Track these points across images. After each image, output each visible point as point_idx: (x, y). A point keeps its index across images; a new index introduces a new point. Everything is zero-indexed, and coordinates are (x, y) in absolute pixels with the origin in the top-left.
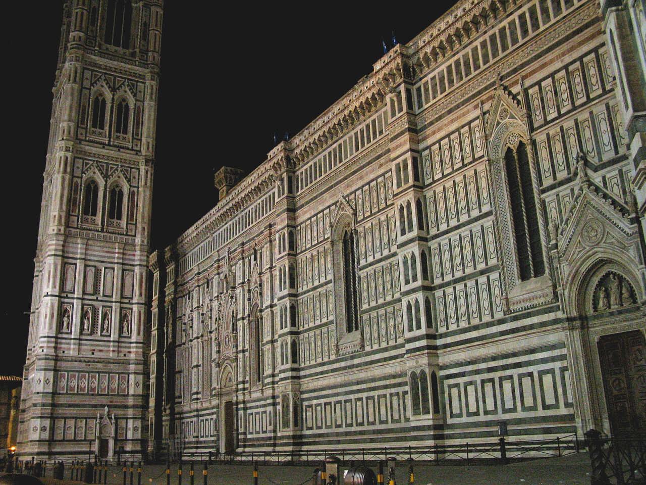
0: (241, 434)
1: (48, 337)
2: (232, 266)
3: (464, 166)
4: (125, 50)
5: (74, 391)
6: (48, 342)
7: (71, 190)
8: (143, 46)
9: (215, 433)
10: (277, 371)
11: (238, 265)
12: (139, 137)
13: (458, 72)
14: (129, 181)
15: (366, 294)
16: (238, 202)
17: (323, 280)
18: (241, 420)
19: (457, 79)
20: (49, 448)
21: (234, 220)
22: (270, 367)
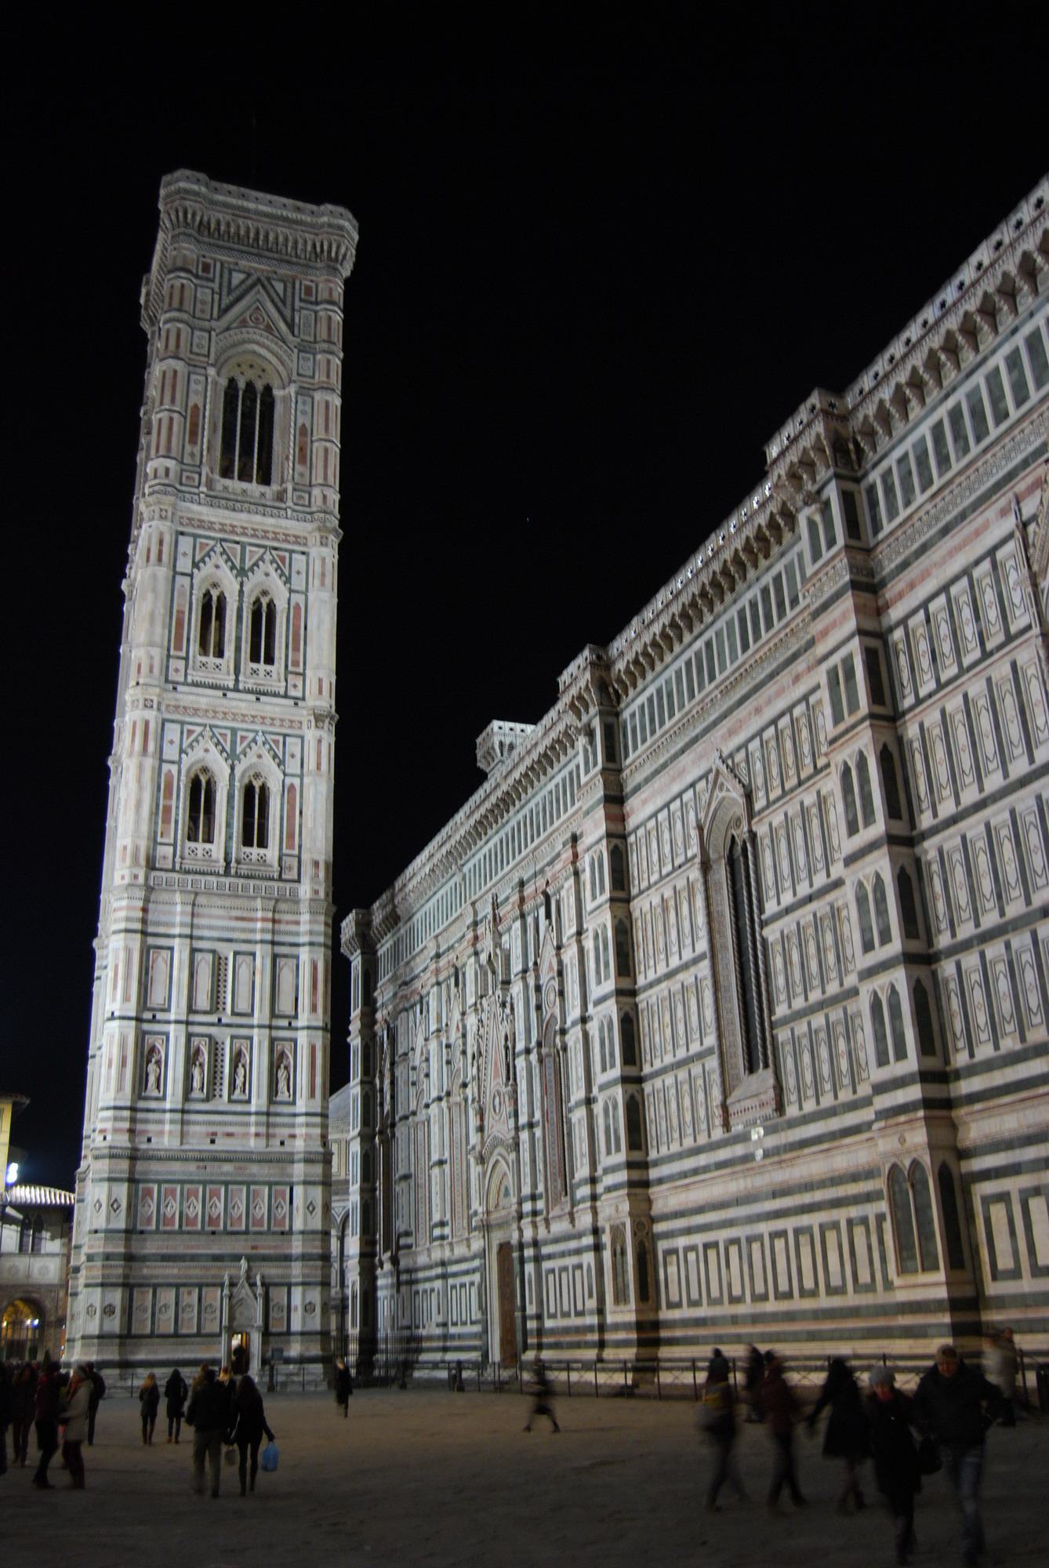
0: (532, 1318)
1: (115, 1108)
2: (501, 935)
3: (986, 655)
5: (174, 1225)
6: (116, 1119)
11: (512, 932)
12: (301, 670)
13: (959, 435)
14: (281, 763)
16: (508, 793)
17: (688, 955)
19: (956, 451)
20: (120, 1354)
21: (502, 833)
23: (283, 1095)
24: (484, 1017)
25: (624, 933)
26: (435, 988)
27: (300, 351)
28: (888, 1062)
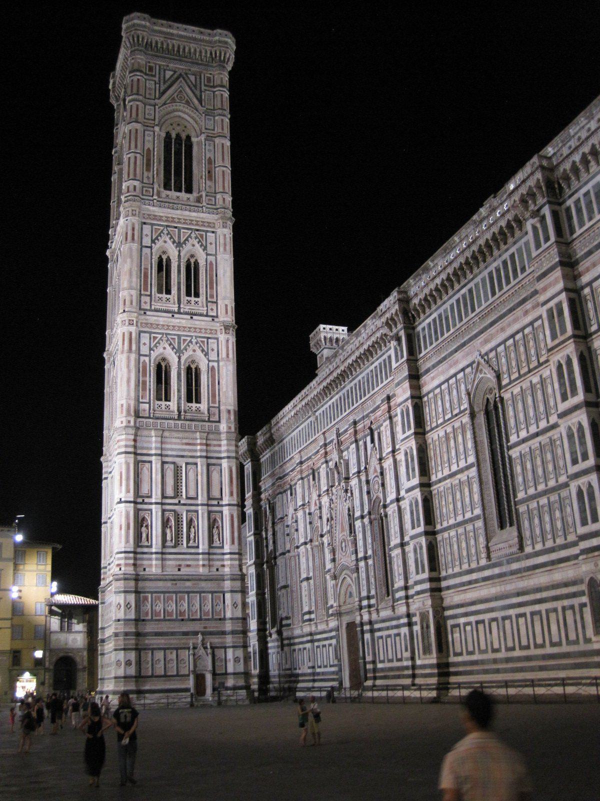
0: (369, 663)
1: (125, 552)
2: (342, 452)
4: (188, 195)
5: (160, 616)
6: (126, 558)
7: (139, 372)
8: (210, 187)
9: (336, 662)
10: (411, 582)
11: (350, 450)
14: (206, 354)
15: (520, 479)
17: (462, 464)
18: (368, 644)
20: (136, 686)
21: (341, 394)
22: (402, 577)
23: (217, 543)
24: (334, 498)
25: (423, 451)
26: (300, 481)
27: (206, 115)
28: (587, 524)
